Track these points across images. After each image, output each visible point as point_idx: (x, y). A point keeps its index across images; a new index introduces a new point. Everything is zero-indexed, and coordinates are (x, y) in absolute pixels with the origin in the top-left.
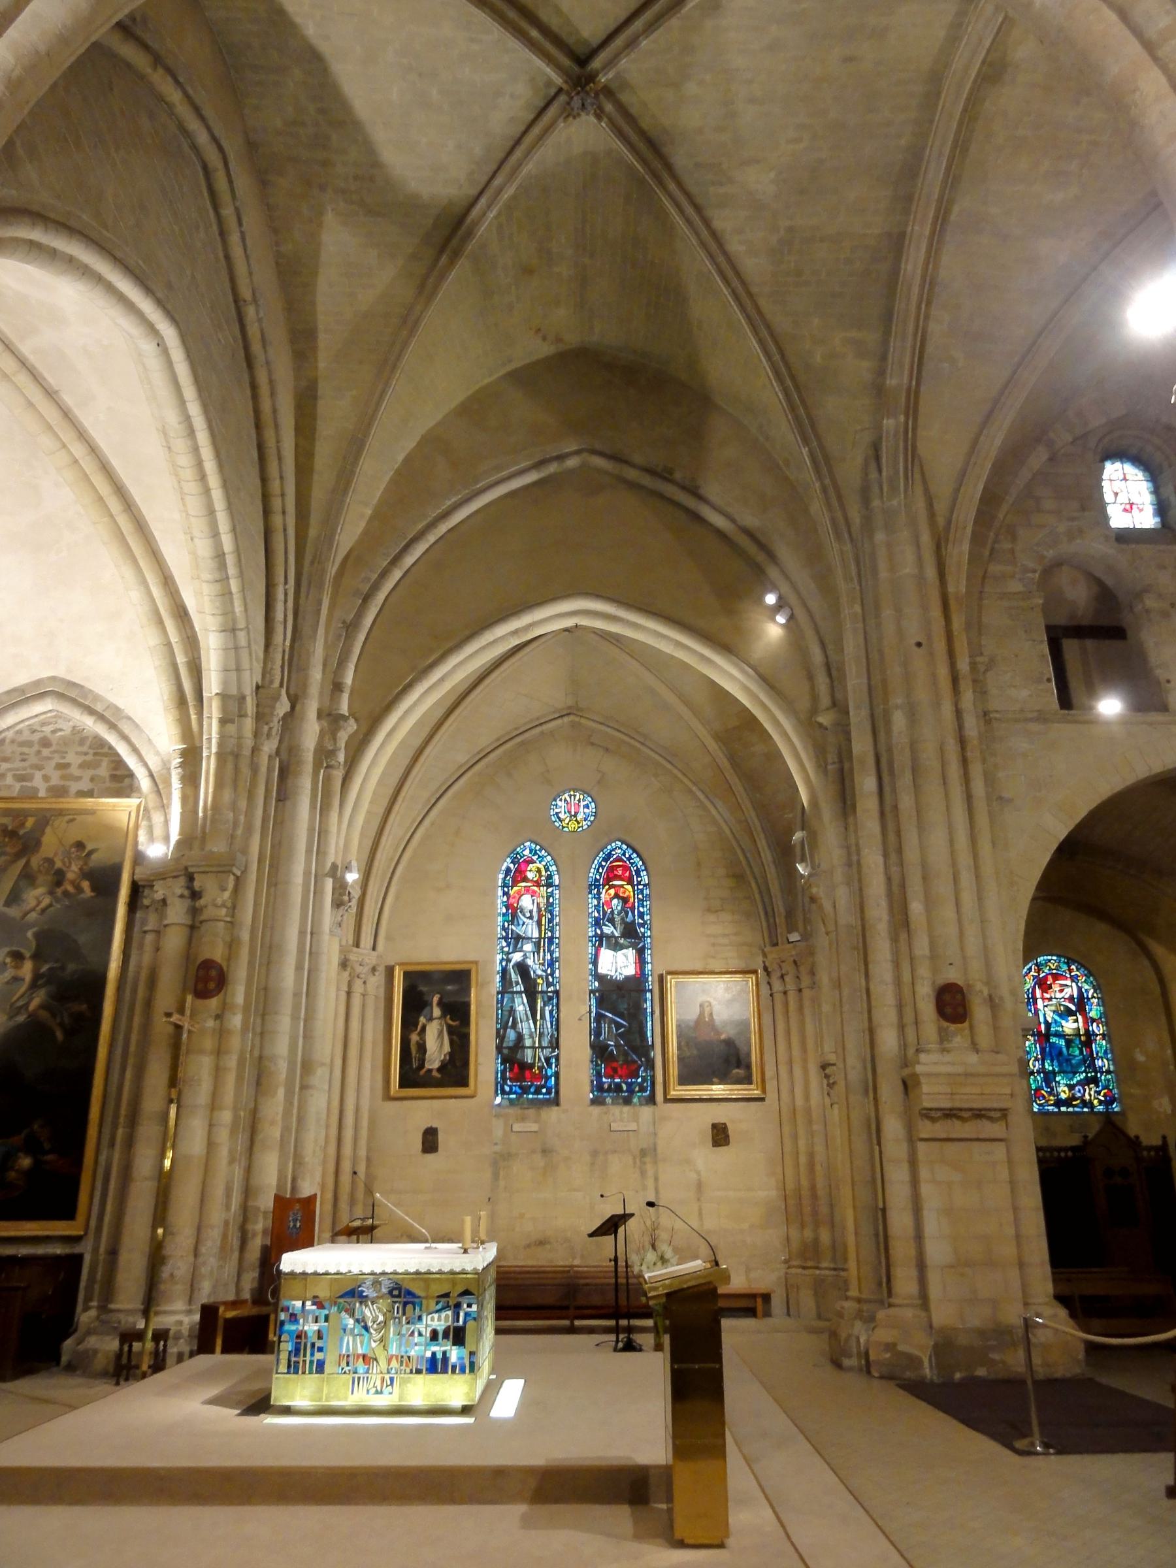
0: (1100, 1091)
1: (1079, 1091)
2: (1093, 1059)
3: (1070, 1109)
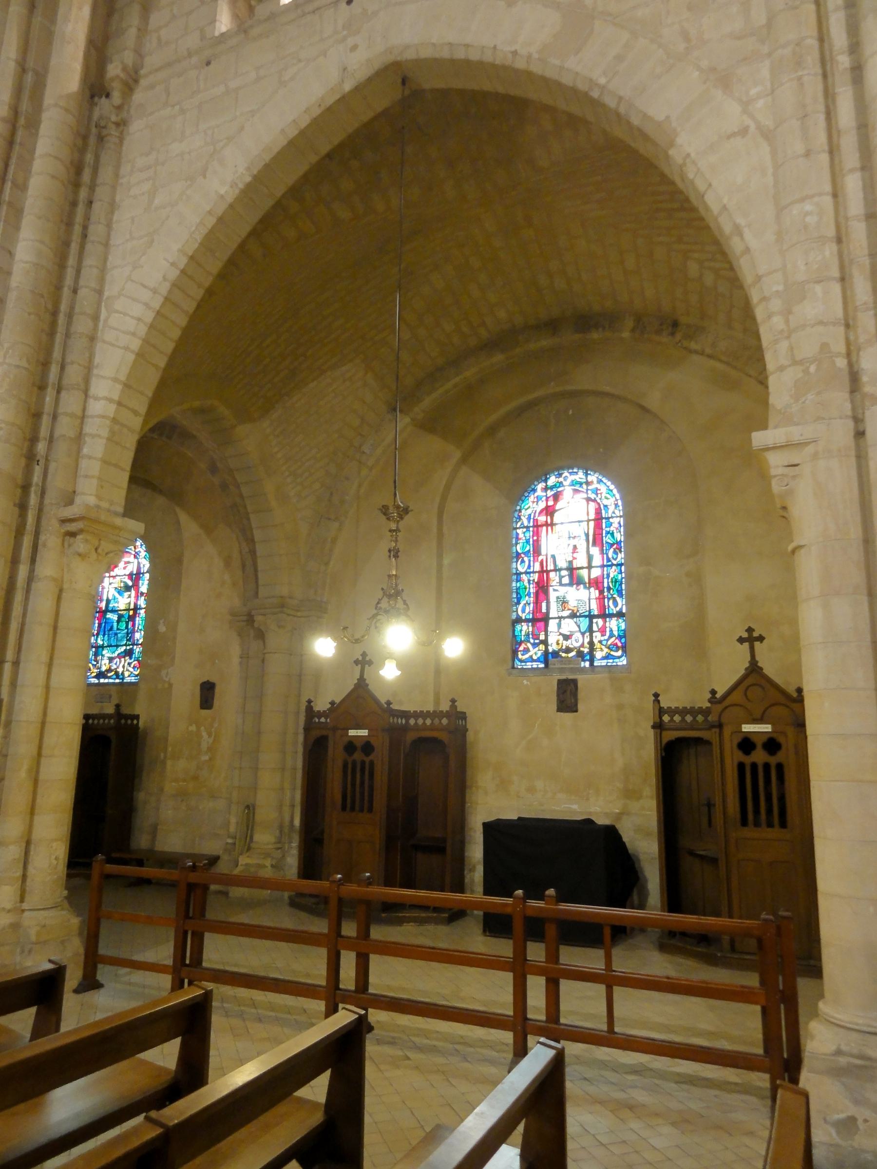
0: (132, 663)
1: (116, 664)
2: (133, 632)
3: (106, 681)
